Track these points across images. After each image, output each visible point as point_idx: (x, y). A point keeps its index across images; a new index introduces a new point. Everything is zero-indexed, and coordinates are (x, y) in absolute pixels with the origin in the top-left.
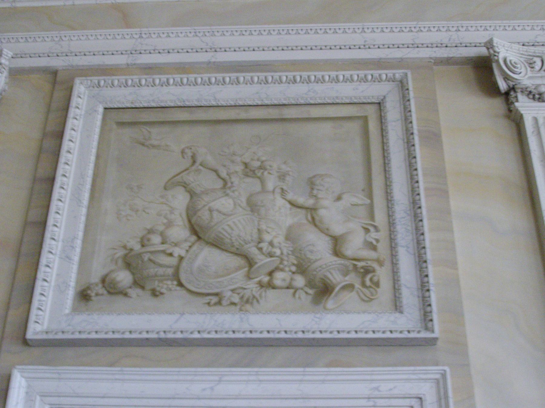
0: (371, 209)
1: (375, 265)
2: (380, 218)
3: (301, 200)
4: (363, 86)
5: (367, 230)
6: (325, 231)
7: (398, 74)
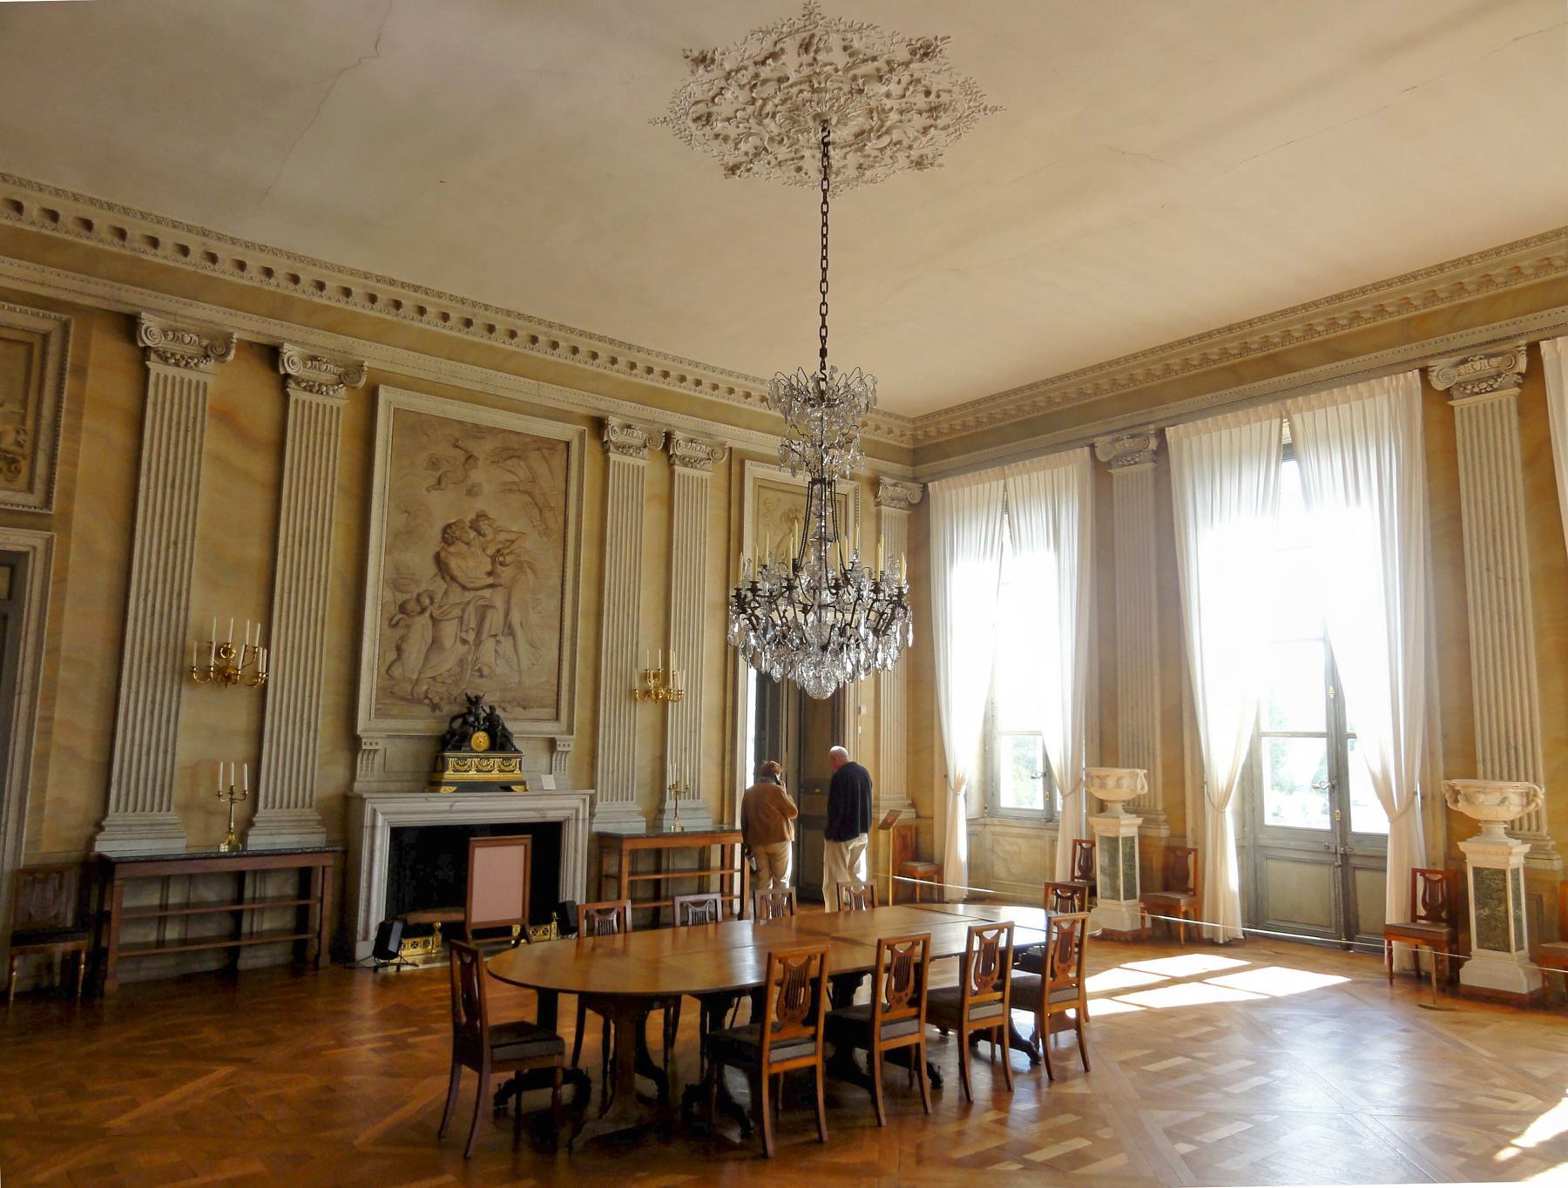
1: (20, 458)
2: (30, 423)
5: (18, 432)
7: (65, 317)
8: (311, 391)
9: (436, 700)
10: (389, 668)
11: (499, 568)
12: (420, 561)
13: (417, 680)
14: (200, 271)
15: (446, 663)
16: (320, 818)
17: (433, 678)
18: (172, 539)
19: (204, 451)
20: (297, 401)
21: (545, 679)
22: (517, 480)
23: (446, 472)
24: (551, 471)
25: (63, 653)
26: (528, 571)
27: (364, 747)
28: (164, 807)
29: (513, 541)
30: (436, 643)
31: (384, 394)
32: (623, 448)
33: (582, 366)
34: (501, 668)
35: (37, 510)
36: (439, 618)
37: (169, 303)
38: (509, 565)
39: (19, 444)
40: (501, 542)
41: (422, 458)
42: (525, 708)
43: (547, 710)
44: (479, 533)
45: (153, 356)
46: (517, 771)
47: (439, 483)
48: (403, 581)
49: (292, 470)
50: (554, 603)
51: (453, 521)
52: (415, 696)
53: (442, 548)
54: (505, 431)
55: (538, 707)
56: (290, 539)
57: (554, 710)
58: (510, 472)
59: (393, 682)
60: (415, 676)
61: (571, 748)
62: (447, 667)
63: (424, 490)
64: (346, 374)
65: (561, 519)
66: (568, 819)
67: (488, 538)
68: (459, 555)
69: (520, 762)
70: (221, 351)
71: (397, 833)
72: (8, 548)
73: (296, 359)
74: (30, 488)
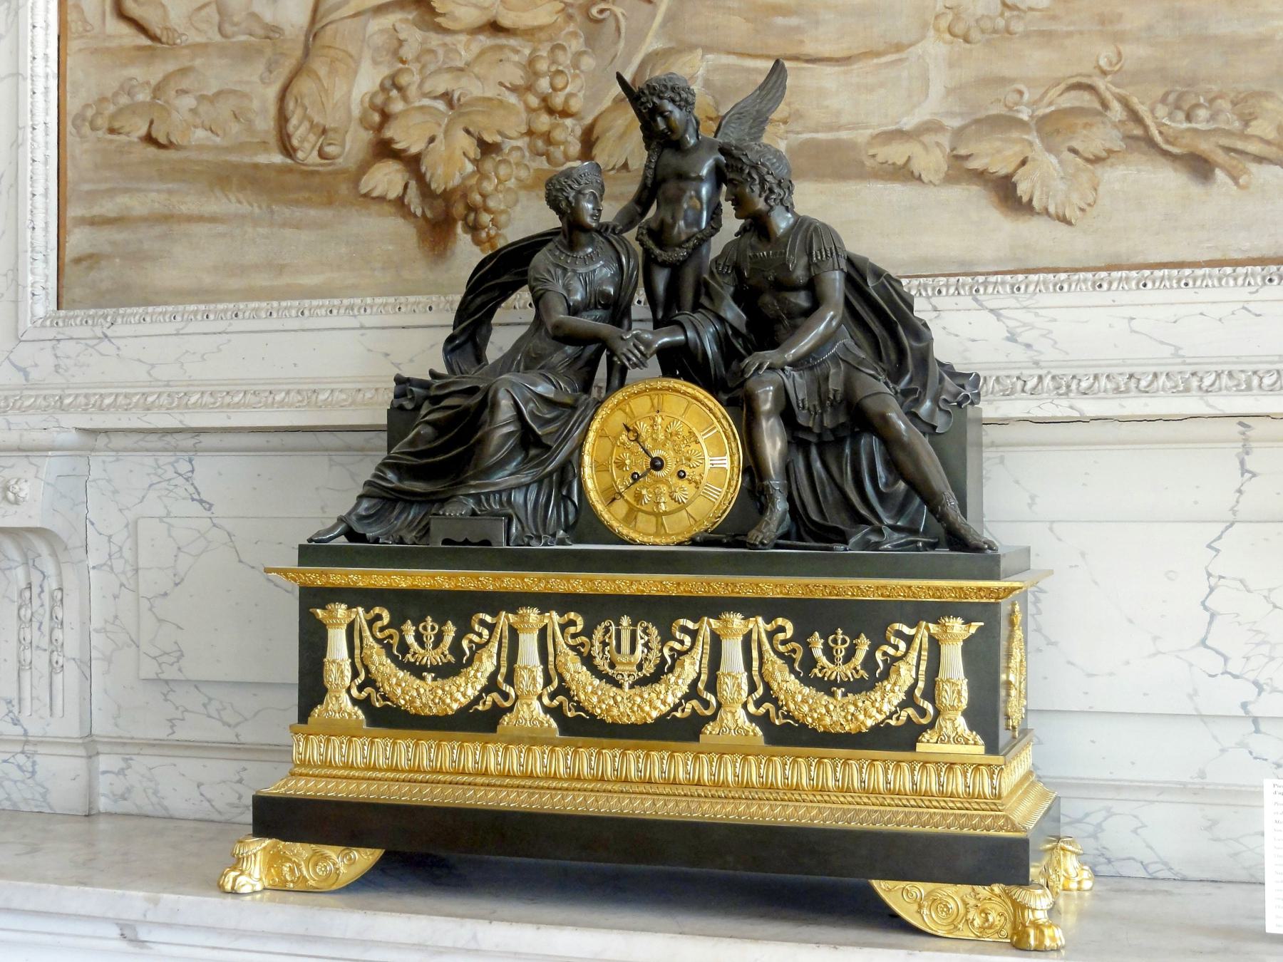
42: (1200, 167)
59: (156, 72)
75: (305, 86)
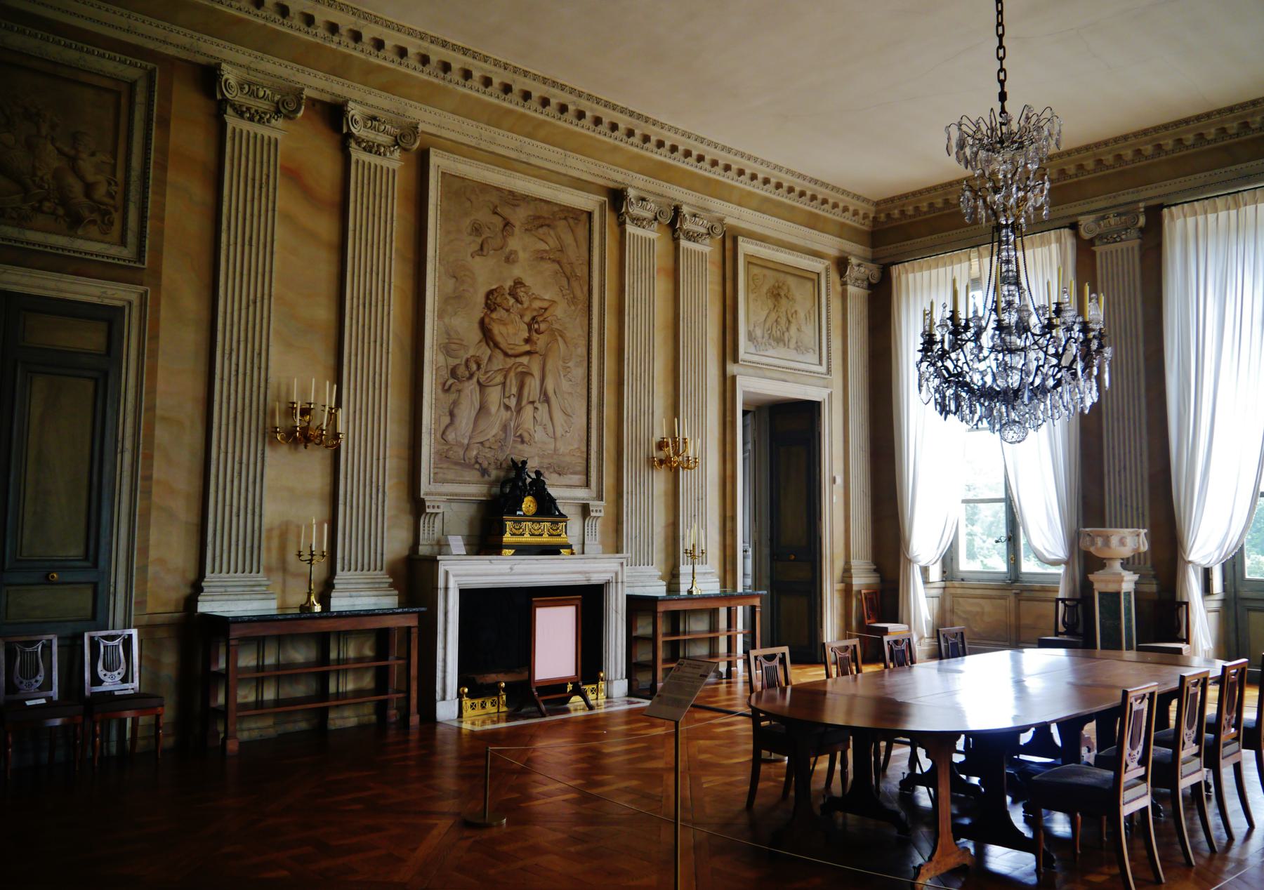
0: (115, 166)
1: (112, 210)
2: (120, 175)
3: (66, 149)
4: (121, 67)
5: (110, 184)
6: (81, 178)
7: (150, 65)
8: (370, 152)
9: (485, 465)
10: (444, 433)
11: (535, 336)
12: (466, 326)
13: (468, 445)
14: (269, 24)
15: (492, 430)
16: (391, 580)
17: (482, 443)
18: (252, 297)
19: (276, 209)
20: (357, 162)
21: (576, 446)
22: (548, 248)
23: (487, 238)
24: (576, 241)
25: (159, 412)
26: (559, 338)
27: (428, 510)
28: (255, 569)
29: (546, 309)
30: (483, 409)
31: (437, 160)
32: (637, 221)
33: (602, 137)
34: (539, 435)
35: (132, 264)
36: (484, 384)
37: (244, 56)
38: (542, 333)
39: (112, 197)
40: (535, 310)
41: (467, 223)
42: (560, 475)
43: (577, 477)
44: (518, 301)
45: (229, 110)
46: (564, 535)
47: (482, 249)
48: (454, 346)
49: (355, 230)
50: (580, 372)
51: (494, 287)
52: (467, 461)
53: (486, 314)
54: (536, 199)
55: (572, 473)
56: (355, 300)
57: (585, 477)
58: (542, 240)
59: (447, 447)
60: (466, 441)
61: (602, 514)
62: (494, 432)
63: (469, 255)
64: (403, 136)
65: (586, 288)
66: (608, 582)
67: (525, 305)
68: (502, 322)
69: (566, 526)
70: (292, 106)
71: (467, 596)
72: (107, 302)
73: (357, 117)
74: (123, 242)
75: (467, 452)
